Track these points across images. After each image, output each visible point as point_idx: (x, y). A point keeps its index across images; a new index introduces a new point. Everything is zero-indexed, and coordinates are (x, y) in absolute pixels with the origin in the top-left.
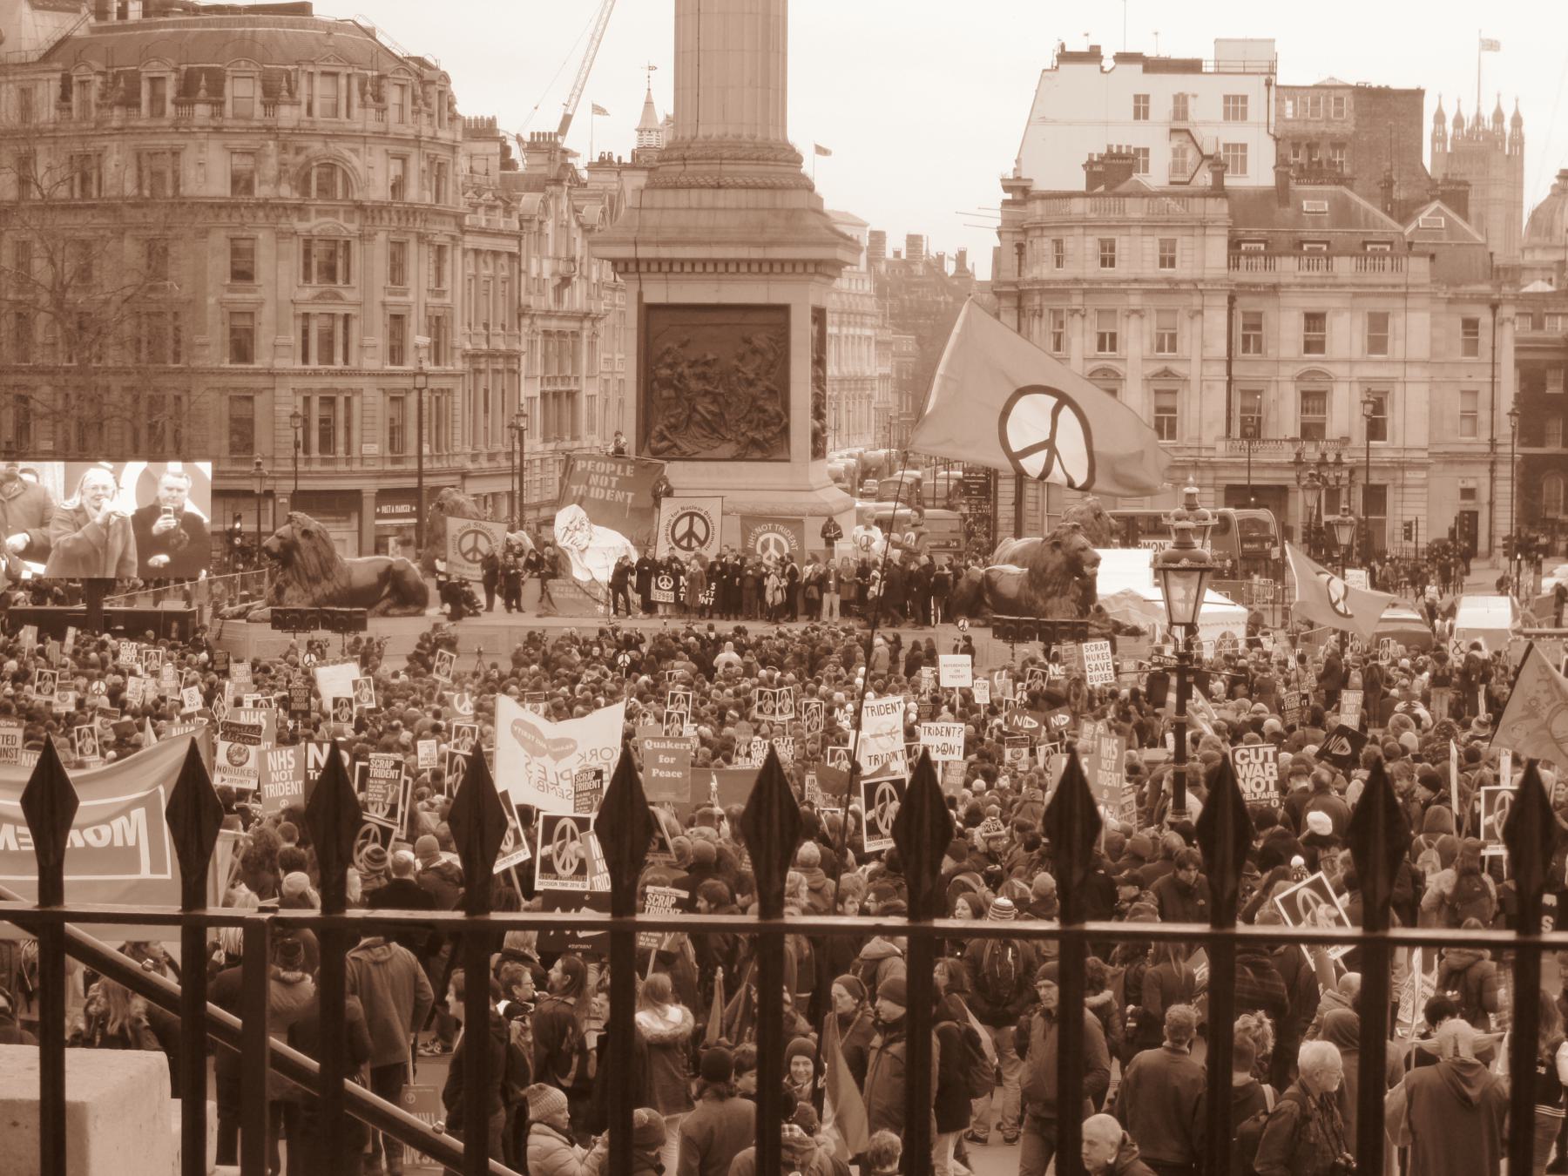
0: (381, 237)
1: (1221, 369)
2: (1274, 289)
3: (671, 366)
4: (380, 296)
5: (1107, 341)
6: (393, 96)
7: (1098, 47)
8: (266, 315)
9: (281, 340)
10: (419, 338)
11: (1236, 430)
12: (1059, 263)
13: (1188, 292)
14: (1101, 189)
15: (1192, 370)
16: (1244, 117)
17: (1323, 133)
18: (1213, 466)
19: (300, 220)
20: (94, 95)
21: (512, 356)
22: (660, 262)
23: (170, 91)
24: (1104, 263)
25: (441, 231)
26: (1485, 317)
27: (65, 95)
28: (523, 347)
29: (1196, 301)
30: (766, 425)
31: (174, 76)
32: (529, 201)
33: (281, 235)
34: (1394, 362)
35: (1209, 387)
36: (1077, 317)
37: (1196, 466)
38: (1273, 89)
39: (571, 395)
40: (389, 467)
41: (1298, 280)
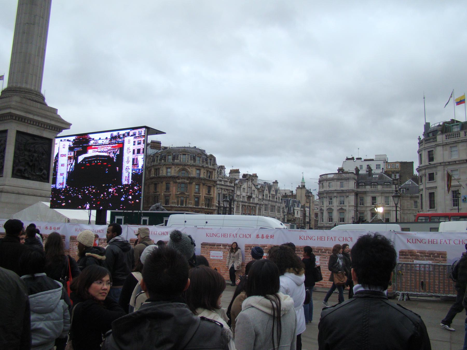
0: (194, 183)
1: (353, 208)
2: (365, 193)
5: (330, 203)
7: (354, 157)
8: (171, 197)
13: (346, 192)
15: (347, 208)
16: (380, 168)
17: (395, 170)
19: (178, 180)
23: (159, 158)
25: (209, 184)
29: (347, 194)
31: (160, 156)
35: (350, 211)
36: (325, 198)
38: (385, 163)
41: (370, 190)
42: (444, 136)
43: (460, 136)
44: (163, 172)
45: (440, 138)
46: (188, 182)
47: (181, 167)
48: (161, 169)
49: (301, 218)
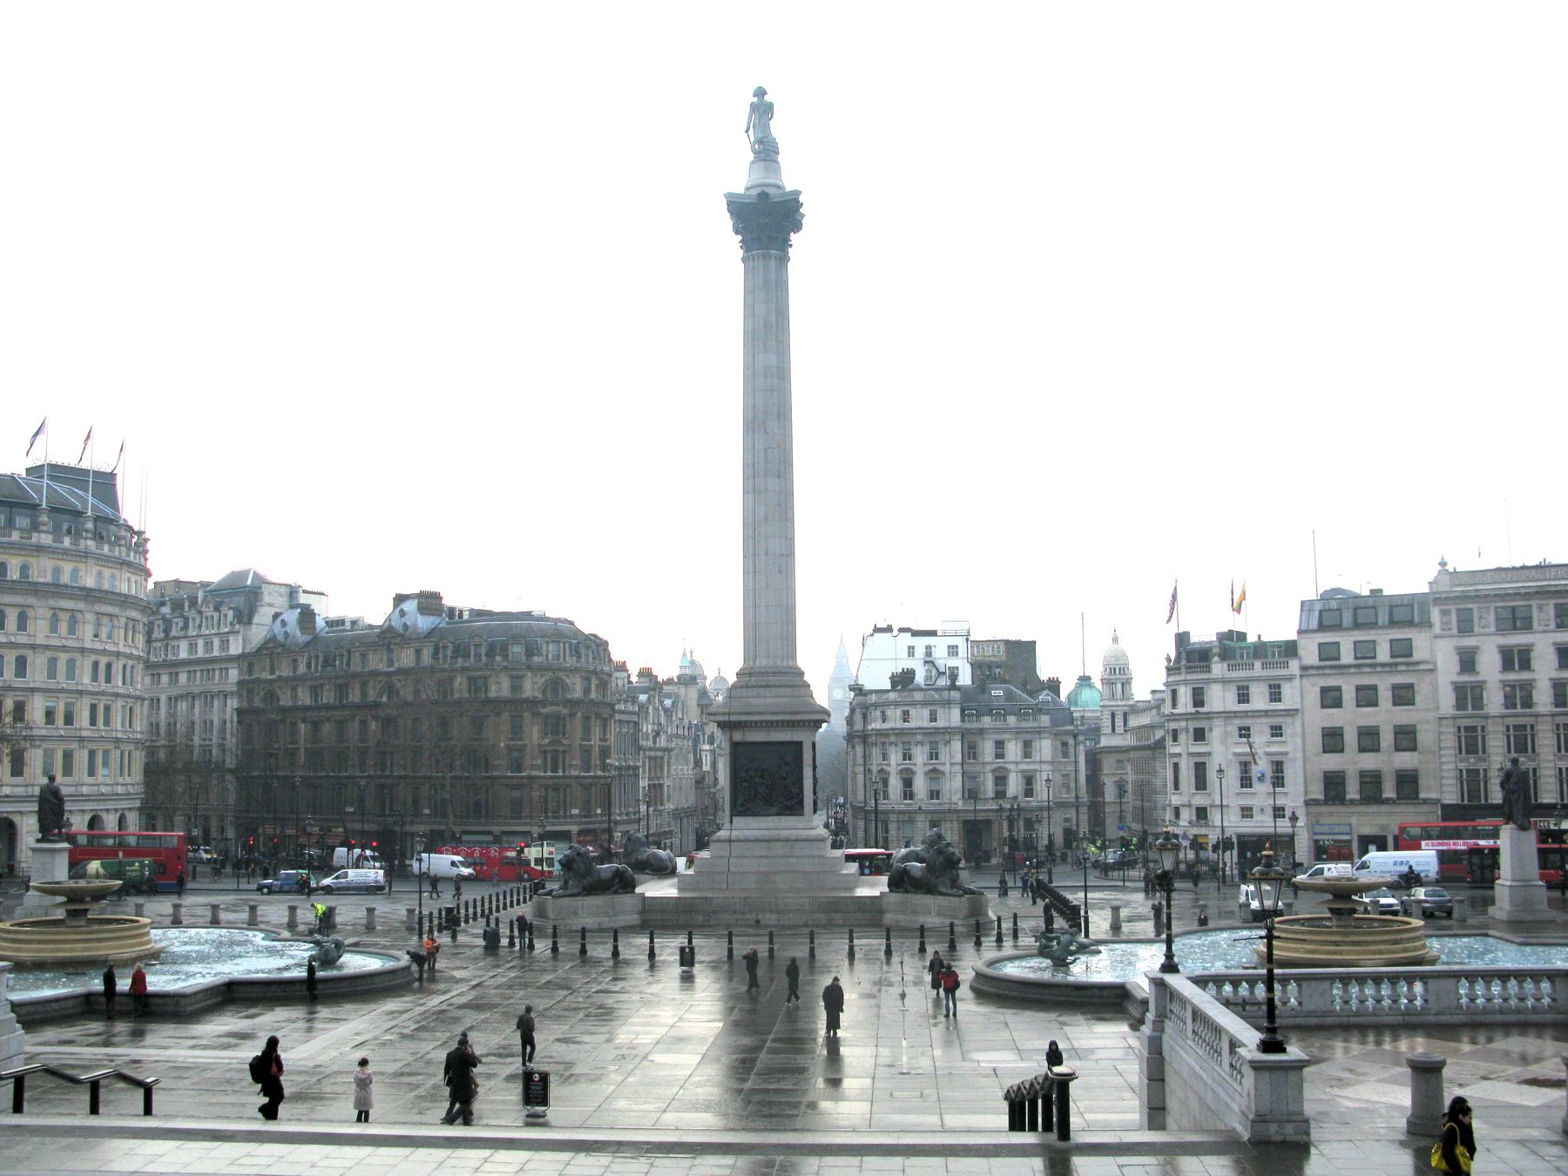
0: (579, 715)
1: (958, 768)
2: (981, 732)
3: (747, 771)
4: (578, 743)
5: (907, 756)
6: (583, 650)
8: (528, 750)
9: (535, 762)
10: (595, 760)
11: (966, 795)
13: (943, 733)
14: (900, 687)
15: (947, 768)
18: (957, 811)
19: (543, 707)
20: (449, 653)
21: (636, 768)
22: (740, 722)
23: (483, 651)
25: (605, 712)
26: (1071, 742)
27: (436, 652)
28: (640, 764)
29: (947, 737)
30: (792, 798)
32: (643, 698)
33: (536, 714)
37: (949, 811)
39: (661, 786)
40: (583, 820)
44: (500, 687)
45: (1218, 668)
46: (565, 711)
47: (549, 675)
48: (492, 680)
49: (711, 771)
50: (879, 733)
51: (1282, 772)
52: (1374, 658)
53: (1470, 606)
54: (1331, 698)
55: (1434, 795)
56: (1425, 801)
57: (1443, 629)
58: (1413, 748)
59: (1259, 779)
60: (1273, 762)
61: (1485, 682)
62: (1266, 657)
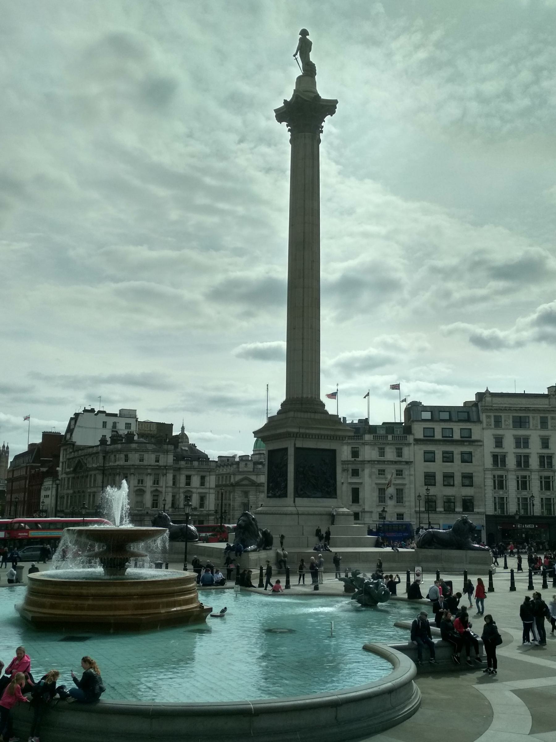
1: (170, 489)
2: (179, 469)
7: (94, 409)
12: (126, 460)
13: (163, 469)
15: (163, 490)
17: (149, 433)
22: (303, 434)
24: (140, 461)
29: (165, 471)
34: (207, 488)
35: (168, 494)
36: (132, 475)
41: (185, 467)
42: (372, 436)
43: (387, 439)
50: (122, 467)
51: (402, 494)
52: (452, 437)
53: (501, 414)
54: (429, 458)
55: (481, 510)
56: (478, 513)
57: (487, 425)
58: (472, 486)
59: (390, 498)
60: (397, 489)
61: (507, 453)
62: (394, 433)
